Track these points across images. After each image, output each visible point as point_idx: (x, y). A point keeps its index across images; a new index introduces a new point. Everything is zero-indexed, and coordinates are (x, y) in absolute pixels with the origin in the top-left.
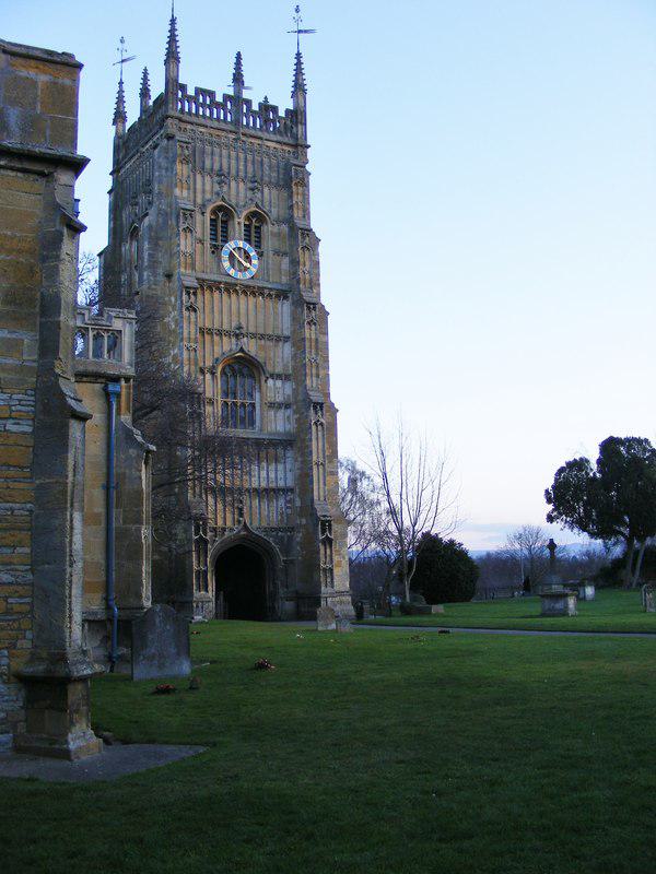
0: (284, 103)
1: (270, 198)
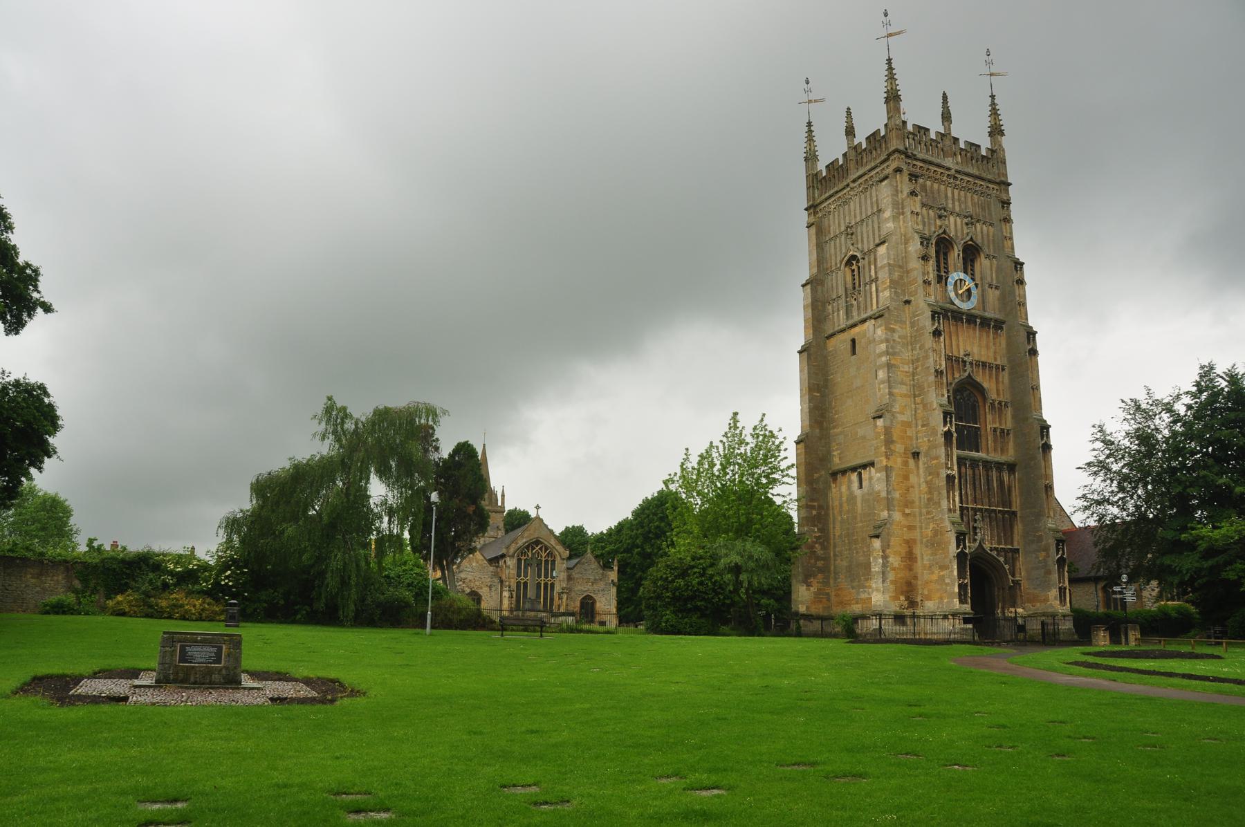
0: (985, 143)
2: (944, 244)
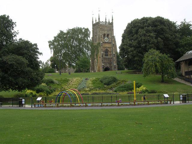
0: (111, 21)
1: (109, 32)
2: (104, 35)
